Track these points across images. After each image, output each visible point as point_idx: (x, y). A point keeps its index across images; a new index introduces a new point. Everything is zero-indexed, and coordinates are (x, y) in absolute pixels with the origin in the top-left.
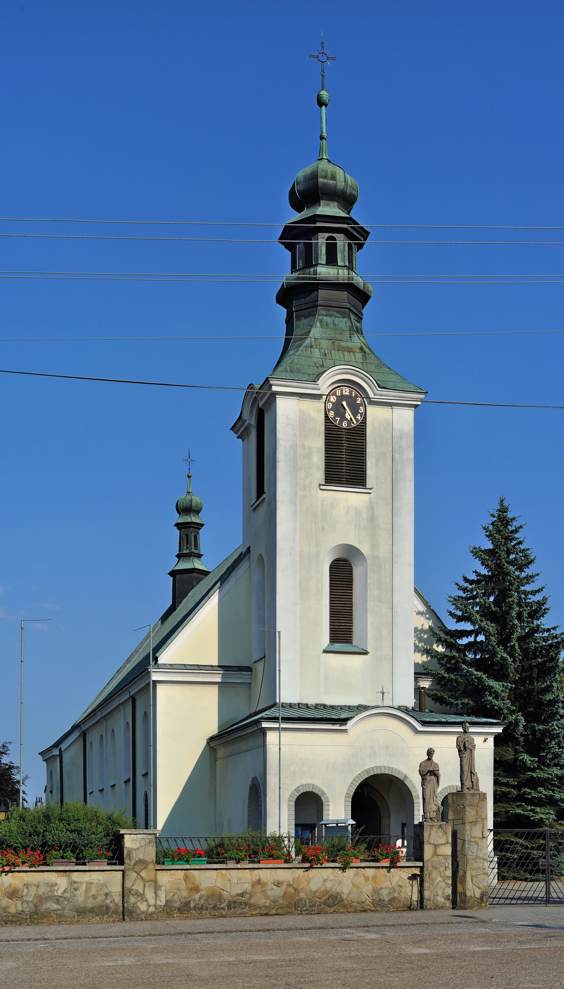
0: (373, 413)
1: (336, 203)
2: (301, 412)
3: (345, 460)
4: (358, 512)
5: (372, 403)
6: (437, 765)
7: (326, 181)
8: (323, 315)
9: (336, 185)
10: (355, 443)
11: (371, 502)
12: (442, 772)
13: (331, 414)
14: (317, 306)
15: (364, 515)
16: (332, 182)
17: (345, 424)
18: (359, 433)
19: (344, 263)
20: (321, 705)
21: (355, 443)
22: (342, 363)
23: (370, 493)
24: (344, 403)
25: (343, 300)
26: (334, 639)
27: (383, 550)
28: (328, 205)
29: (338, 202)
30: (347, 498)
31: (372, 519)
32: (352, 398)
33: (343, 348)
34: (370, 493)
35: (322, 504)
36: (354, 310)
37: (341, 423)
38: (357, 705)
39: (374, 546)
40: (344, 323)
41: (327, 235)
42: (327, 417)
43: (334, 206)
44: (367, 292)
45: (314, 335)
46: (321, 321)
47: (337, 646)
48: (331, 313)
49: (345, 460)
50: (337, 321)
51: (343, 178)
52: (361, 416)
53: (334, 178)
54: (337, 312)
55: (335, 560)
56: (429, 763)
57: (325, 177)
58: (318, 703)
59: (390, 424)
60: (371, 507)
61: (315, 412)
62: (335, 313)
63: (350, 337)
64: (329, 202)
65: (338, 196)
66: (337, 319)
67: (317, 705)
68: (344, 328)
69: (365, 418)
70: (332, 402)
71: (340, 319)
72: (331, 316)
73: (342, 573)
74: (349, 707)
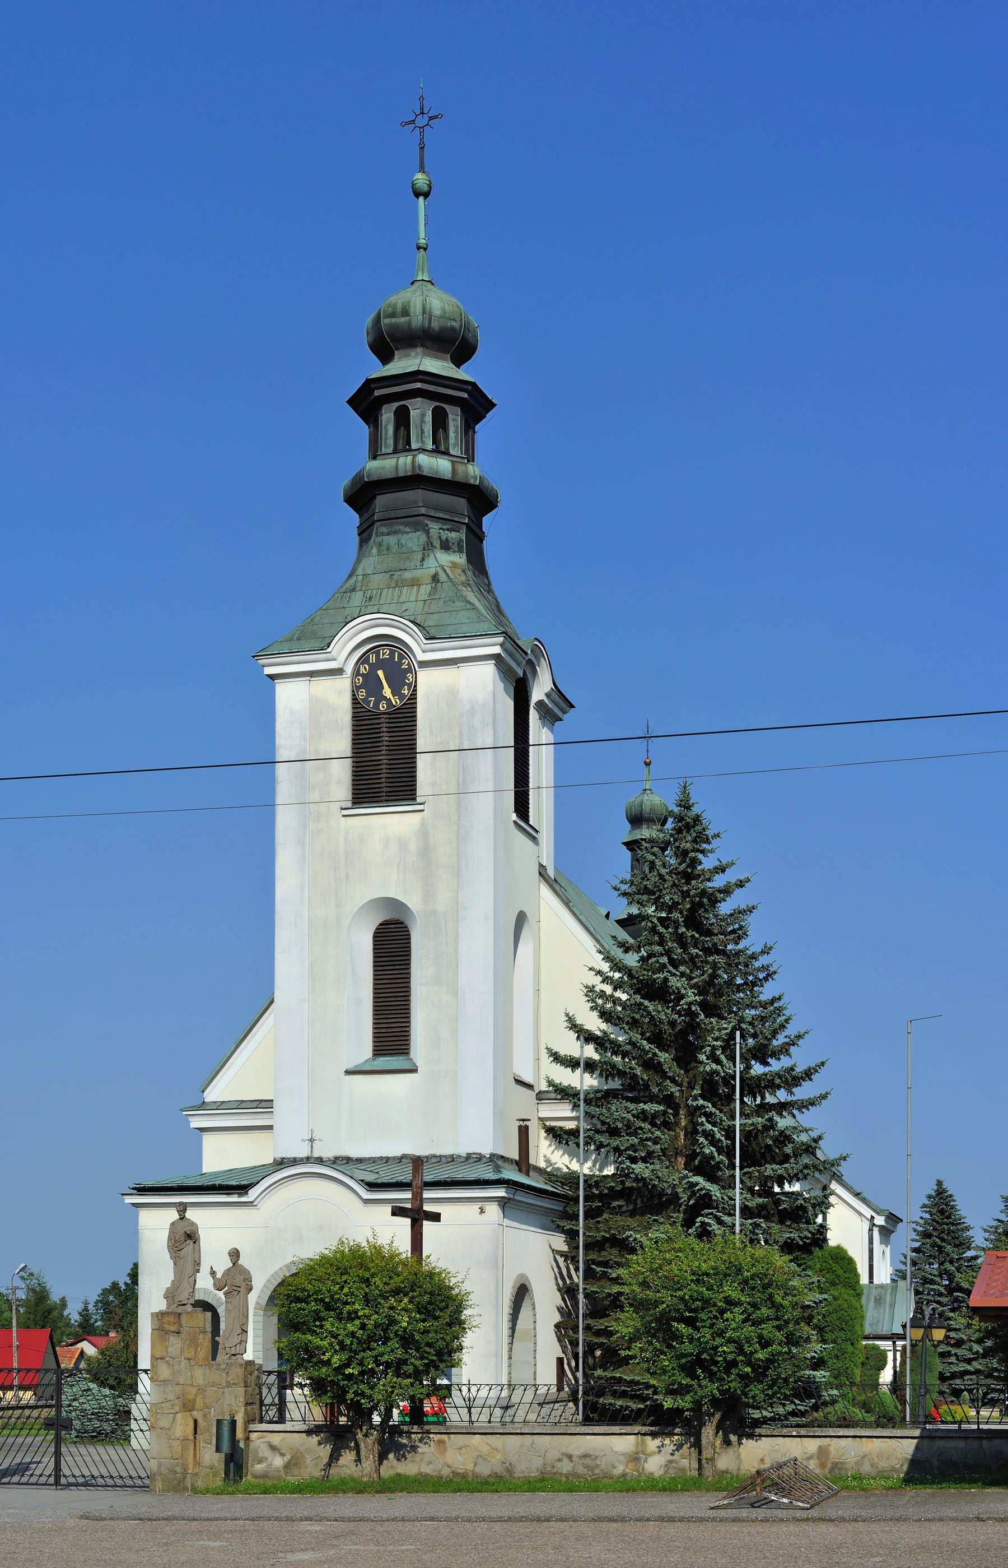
0: (427, 681)
1: (419, 350)
2: (312, 698)
3: (384, 763)
4: (403, 844)
5: (423, 664)
6: (193, 1224)
7: (393, 320)
8: (383, 534)
9: (409, 323)
10: (402, 734)
11: (423, 824)
12: (202, 1233)
13: (362, 694)
14: (373, 523)
15: (413, 847)
16: (403, 320)
17: (383, 707)
18: (405, 717)
19: (423, 442)
20: (343, 1158)
21: (402, 734)
22: (392, 608)
23: (423, 811)
24: (380, 673)
25: (416, 502)
26: (379, 1051)
27: (442, 901)
28: (408, 356)
29: (423, 345)
30: (390, 824)
31: (426, 852)
32: (386, 667)
33: (404, 581)
34: (423, 811)
35: (346, 839)
36: (441, 515)
37: (376, 704)
38: (399, 1155)
39: (428, 895)
40: (416, 540)
41: (395, 405)
42: (355, 700)
43: (417, 355)
44: (463, 481)
45: (363, 570)
46: (380, 545)
47: (383, 1062)
48: (396, 528)
49: (384, 763)
50: (404, 539)
51: (432, 302)
52: (409, 690)
53: (405, 312)
54: (406, 525)
55: (381, 924)
56: (182, 1223)
57: (393, 315)
58: (338, 1155)
59: (458, 693)
60: (424, 832)
61: (337, 696)
62: (402, 528)
63: (423, 560)
64: (409, 351)
65: (419, 338)
66: (405, 535)
67: (336, 1158)
68: (415, 548)
69: (415, 690)
70: (363, 675)
71: (410, 535)
72: (396, 532)
73: (392, 945)
74: (387, 1159)
